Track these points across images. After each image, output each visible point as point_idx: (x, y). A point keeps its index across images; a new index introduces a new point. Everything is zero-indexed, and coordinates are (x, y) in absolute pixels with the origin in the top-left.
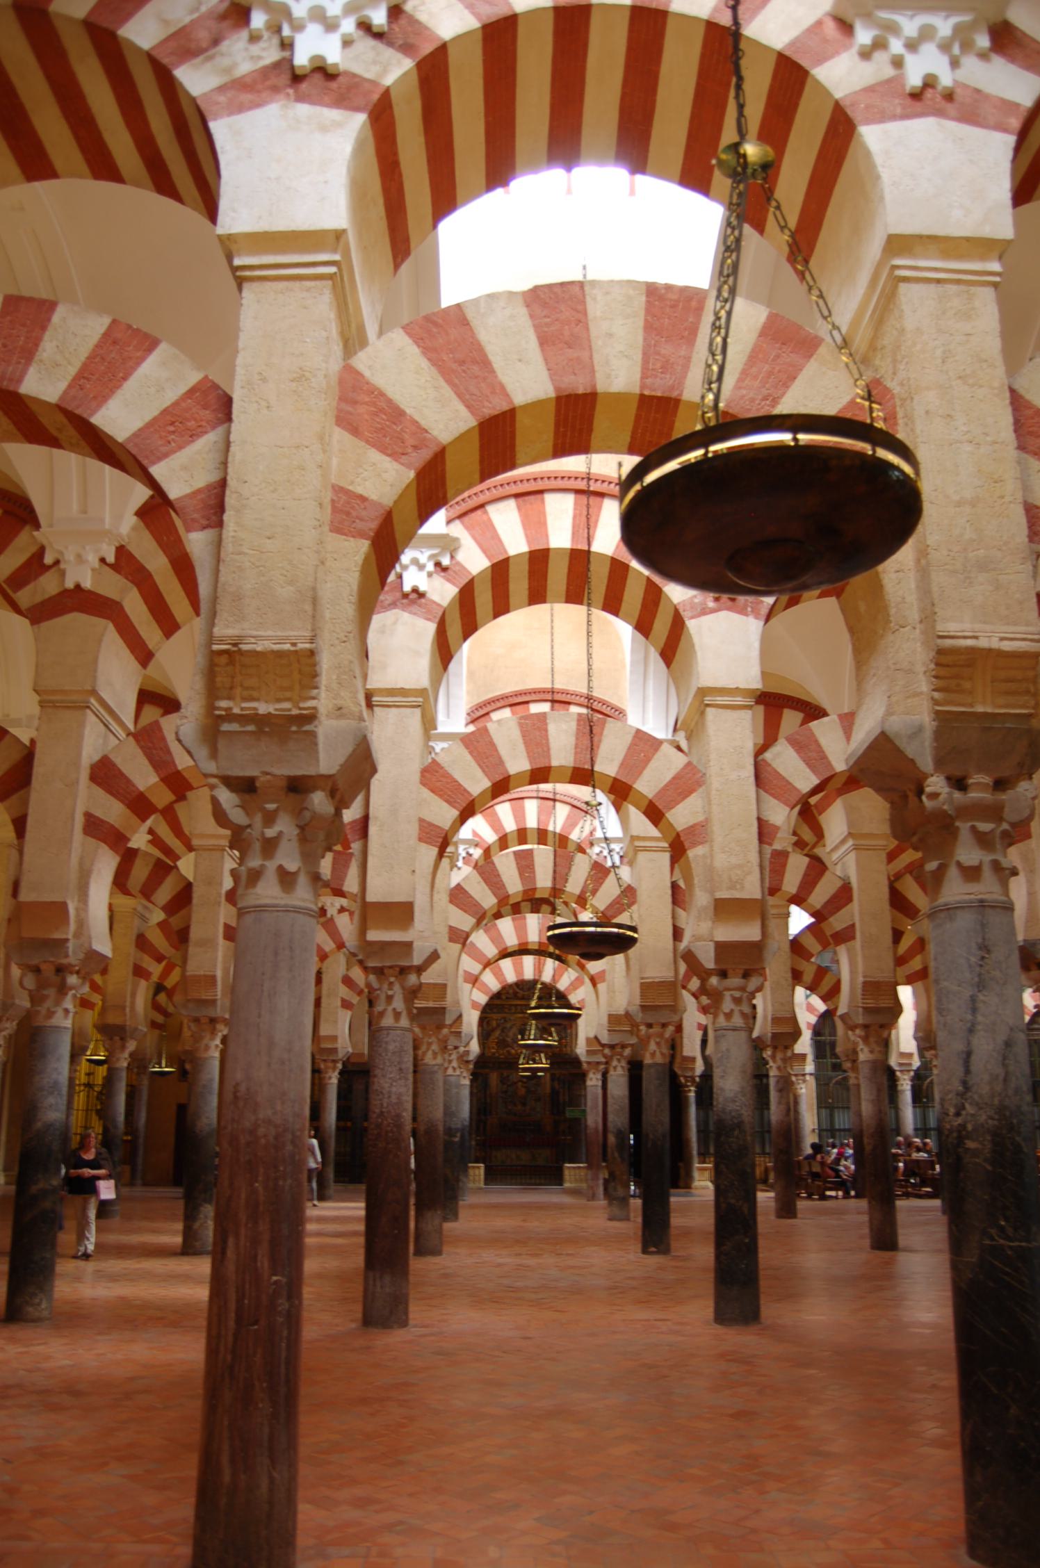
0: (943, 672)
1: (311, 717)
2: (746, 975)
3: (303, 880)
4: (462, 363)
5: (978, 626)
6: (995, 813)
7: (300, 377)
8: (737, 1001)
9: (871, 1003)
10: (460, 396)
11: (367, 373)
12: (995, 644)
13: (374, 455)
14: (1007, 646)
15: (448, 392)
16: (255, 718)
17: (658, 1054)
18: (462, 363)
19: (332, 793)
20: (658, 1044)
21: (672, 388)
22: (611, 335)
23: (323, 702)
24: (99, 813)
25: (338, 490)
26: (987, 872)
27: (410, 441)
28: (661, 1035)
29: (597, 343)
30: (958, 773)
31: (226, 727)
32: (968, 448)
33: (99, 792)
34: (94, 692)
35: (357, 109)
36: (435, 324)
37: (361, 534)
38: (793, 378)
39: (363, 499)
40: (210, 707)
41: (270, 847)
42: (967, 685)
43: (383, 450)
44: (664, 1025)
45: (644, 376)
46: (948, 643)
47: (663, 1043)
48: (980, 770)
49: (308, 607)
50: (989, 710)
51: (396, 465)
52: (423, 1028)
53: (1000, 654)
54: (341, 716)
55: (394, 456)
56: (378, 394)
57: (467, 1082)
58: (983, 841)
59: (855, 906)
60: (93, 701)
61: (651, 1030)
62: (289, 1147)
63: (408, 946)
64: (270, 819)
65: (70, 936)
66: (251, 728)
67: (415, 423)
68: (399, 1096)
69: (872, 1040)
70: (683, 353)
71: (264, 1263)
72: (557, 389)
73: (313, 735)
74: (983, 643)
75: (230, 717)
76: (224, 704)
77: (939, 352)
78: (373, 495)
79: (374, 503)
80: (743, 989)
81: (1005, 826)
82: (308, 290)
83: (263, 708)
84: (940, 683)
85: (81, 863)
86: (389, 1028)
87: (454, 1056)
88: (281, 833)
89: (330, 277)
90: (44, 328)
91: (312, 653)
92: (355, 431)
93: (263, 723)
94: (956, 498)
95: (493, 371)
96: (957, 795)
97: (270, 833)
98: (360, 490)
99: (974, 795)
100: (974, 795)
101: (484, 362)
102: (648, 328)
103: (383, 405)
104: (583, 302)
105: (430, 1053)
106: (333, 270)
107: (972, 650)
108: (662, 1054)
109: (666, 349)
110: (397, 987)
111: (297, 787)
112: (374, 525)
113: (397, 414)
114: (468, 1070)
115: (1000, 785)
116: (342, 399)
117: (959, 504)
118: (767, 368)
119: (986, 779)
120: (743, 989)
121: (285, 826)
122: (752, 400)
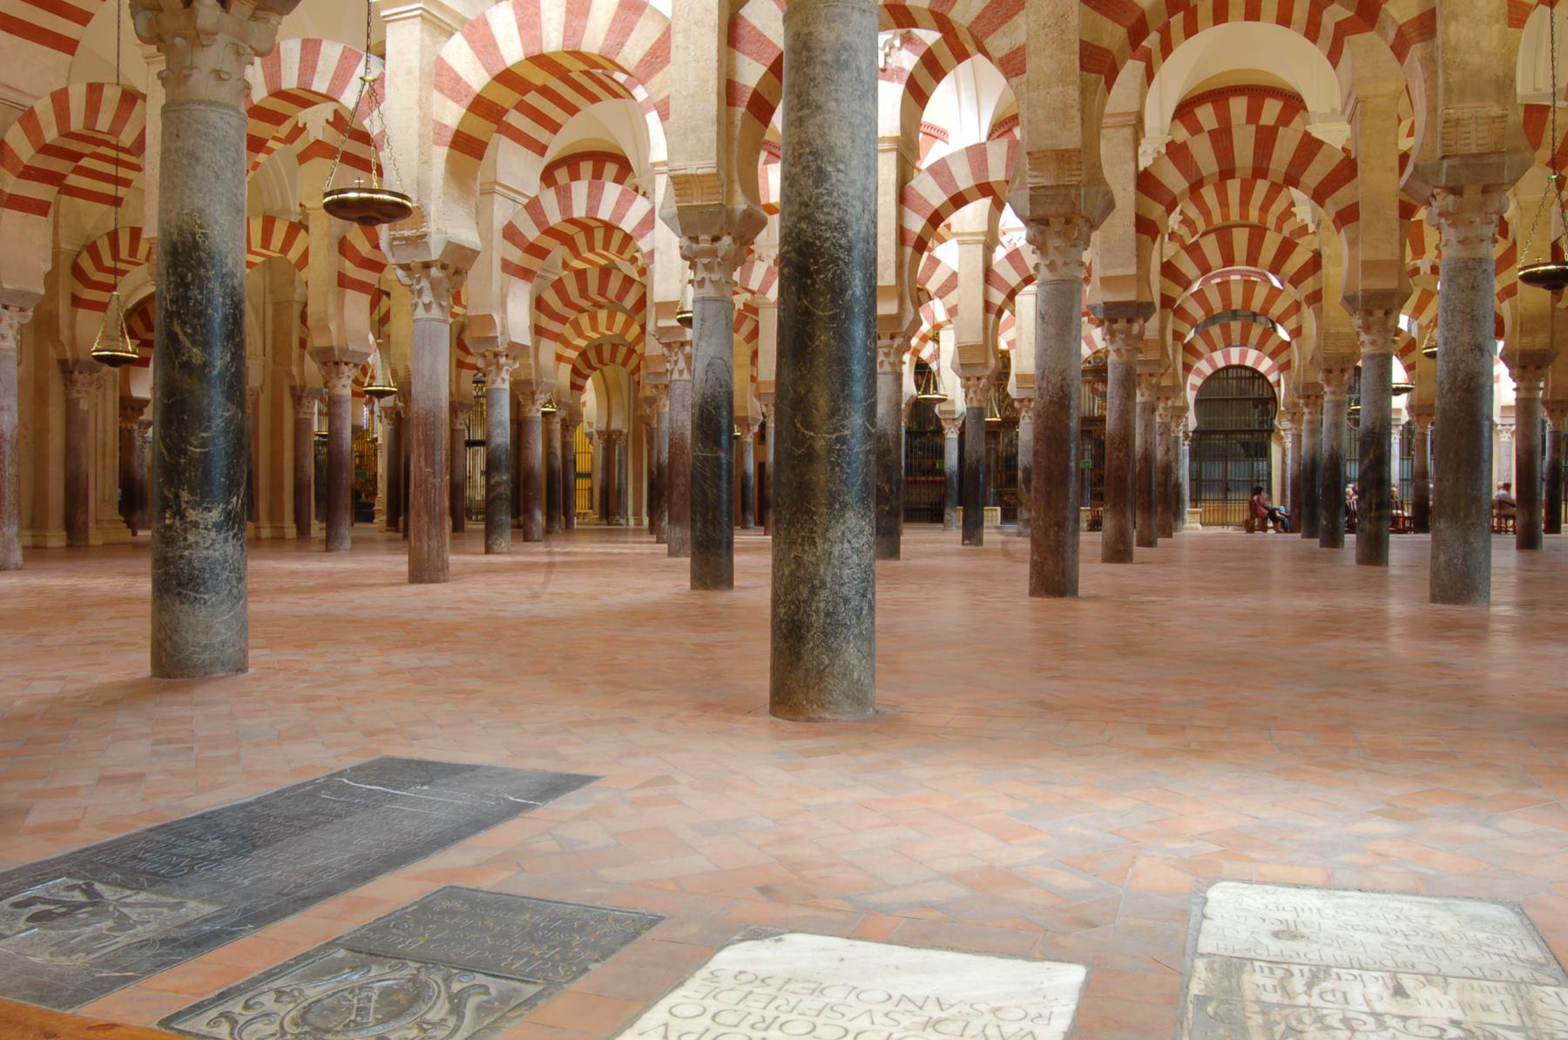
0: (677, 187)
2: (892, 337)
3: (434, 306)
4: (485, 47)
5: (687, 163)
6: (713, 253)
7: (409, 73)
8: (887, 355)
11: (446, 58)
12: (694, 172)
14: (700, 172)
15: (479, 65)
17: (974, 400)
18: (485, 47)
19: (444, 267)
20: (975, 392)
21: (576, 45)
22: (550, 19)
24: (509, 258)
26: (707, 281)
27: (464, 93)
28: (978, 385)
29: (544, 25)
30: (693, 235)
31: (395, 243)
32: (694, 64)
33: (508, 244)
34: (496, 182)
36: (473, 26)
37: (446, 145)
38: (632, 30)
39: (446, 126)
41: (420, 292)
42: (689, 192)
43: (453, 99)
44: (979, 379)
45: (564, 40)
46: (673, 173)
47: (979, 391)
48: (702, 233)
49: (415, 186)
50: (699, 203)
53: (698, 176)
54: (439, 233)
55: (457, 101)
56: (451, 70)
58: (708, 267)
60: (497, 187)
61: (969, 383)
62: (432, 418)
64: (419, 281)
65: (498, 334)
67: (465, 83)
68: (683, 421)
70: (582, 24)
71: (423, 463)
72: (525, 55)
74: (689, 172)
75: (395, 239)
77: (687, 9)
79: (451, 128)
80: (891, 347)
81: (719, 260)
82: (412, 24)
83: (406, 233)
84: (677, 192)
85: (502, 289)
86: (676, 381)
88: (422, 287)
89: (420, 15)
90: (318, 55)
92: (442, 91)
93: (407, 239)
94: (685, 94)
95: (498, 49)
96: (695, 246)
97: (418, 287)
98: (444, 122)
99: (702, 245)
100: (702, 245)
101: (494, 45)
102: (569, 11)
103: (452, 75)
106: (419, 12)
107: (685, 175)
108: (978, 400)
109: (575, 23)
110: (680, 355)
111: (427, 266)
113: (458, 79)
114: (955, 427)
115: (715, 239)
117: (686, 97)
118: (620, 26)
119: (708, 238)
120: (891, 347)
121: (425, 283)
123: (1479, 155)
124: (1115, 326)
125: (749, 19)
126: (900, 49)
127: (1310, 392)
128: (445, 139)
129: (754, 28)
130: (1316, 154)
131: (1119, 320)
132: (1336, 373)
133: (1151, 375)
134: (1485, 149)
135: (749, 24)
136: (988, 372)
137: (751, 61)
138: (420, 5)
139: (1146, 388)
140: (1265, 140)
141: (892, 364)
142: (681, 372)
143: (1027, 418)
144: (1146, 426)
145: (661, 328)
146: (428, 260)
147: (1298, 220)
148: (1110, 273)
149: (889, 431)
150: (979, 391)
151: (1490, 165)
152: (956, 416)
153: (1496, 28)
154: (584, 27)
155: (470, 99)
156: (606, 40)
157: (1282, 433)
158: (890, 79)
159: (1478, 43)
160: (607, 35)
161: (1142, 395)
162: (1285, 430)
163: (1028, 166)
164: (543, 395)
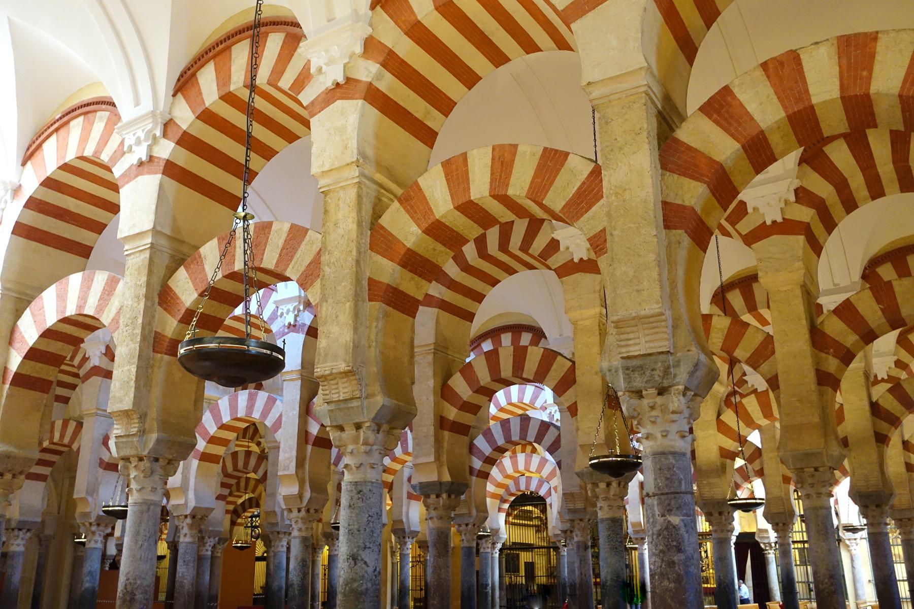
9: (571, 506)
20: (465, 534)
28: (467, 530)
44: (467, 525)
47: (468, 534)
123: (346, 400)
126: (304, 311)
127: (777, 521)
130: (552, 364)
132: (716, 515)
133: (581, 520)
134: (347, 396)
136: (472, 520)
139: (579, 529)
140: (520, 355)
141: (300, 530)
143: (570, 545)
144: (581, 561)
147: (750, 385)
148: (419, 461)
149: (295, 582)
150: (468, 534)
151: (352, 407)
153: (348, 304)
157: (847, 542)
158: (298, 332)
159: (337, 317)
162: (849, 540)
164: (212, 539)
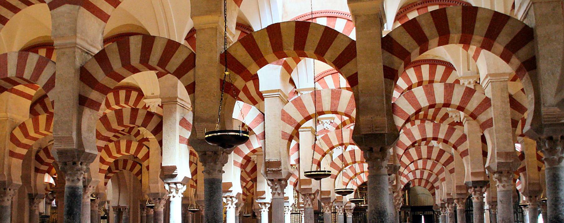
1: (281, 170)
10: (301, 114)
13: (288, 125)
16: (272, 171)
23: (282, 167)
25: (282, 132)
31: (269, 172)
35: (280, 65)
36: (296, 100)
37: (286, 139)
40: (266, 169)
41: (276, 189)
45: (331, 106)
51: (291, 127)
52: (324, 203)
55: (291, 125)
57: (351, 216)
59: (453, 163)
63: (311, 188)
64: (276, 185)
66: (272, 172)
69: (460, 203)
73: (281, 173)
75: (269, 171)
76: (268, 169)
78: (288, 132)
79: (288, 134)
83: (274, 169)
87: (341, 209)
91: (280, 161)
92: (284, 121)
97: (276, 187)
102: (332, 98)
104: (321, 94)
105: (327, 210)
110: (309, 199)
111: (280, 180)
112: (288, 138)
113: (291, 117)
116: (282, 115)
118: (352, 104)
122: (349, 111)
124: (476, 189)
125: (398, 105)
128: (286, 138)
129: (400, 108)
131: (478, 187)
135: (398, 106)
137: (399, 118)
138: (279, 93)
142: (309, 205)
145: (302, 188)
146: (281, 178)
148: (474, 171)
152: (352, 208)
154: (338, 103)
155: (296, 125)
156: (347, 108)
160: (347, 107)
161: (460, 206)
163: (496, 156)
